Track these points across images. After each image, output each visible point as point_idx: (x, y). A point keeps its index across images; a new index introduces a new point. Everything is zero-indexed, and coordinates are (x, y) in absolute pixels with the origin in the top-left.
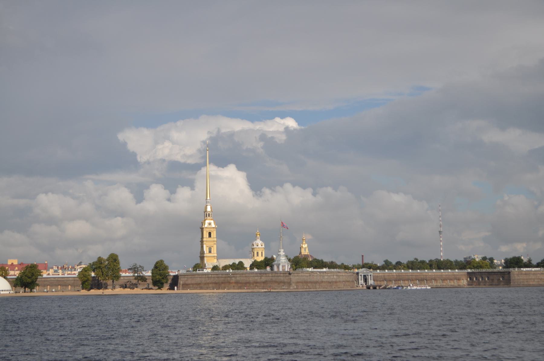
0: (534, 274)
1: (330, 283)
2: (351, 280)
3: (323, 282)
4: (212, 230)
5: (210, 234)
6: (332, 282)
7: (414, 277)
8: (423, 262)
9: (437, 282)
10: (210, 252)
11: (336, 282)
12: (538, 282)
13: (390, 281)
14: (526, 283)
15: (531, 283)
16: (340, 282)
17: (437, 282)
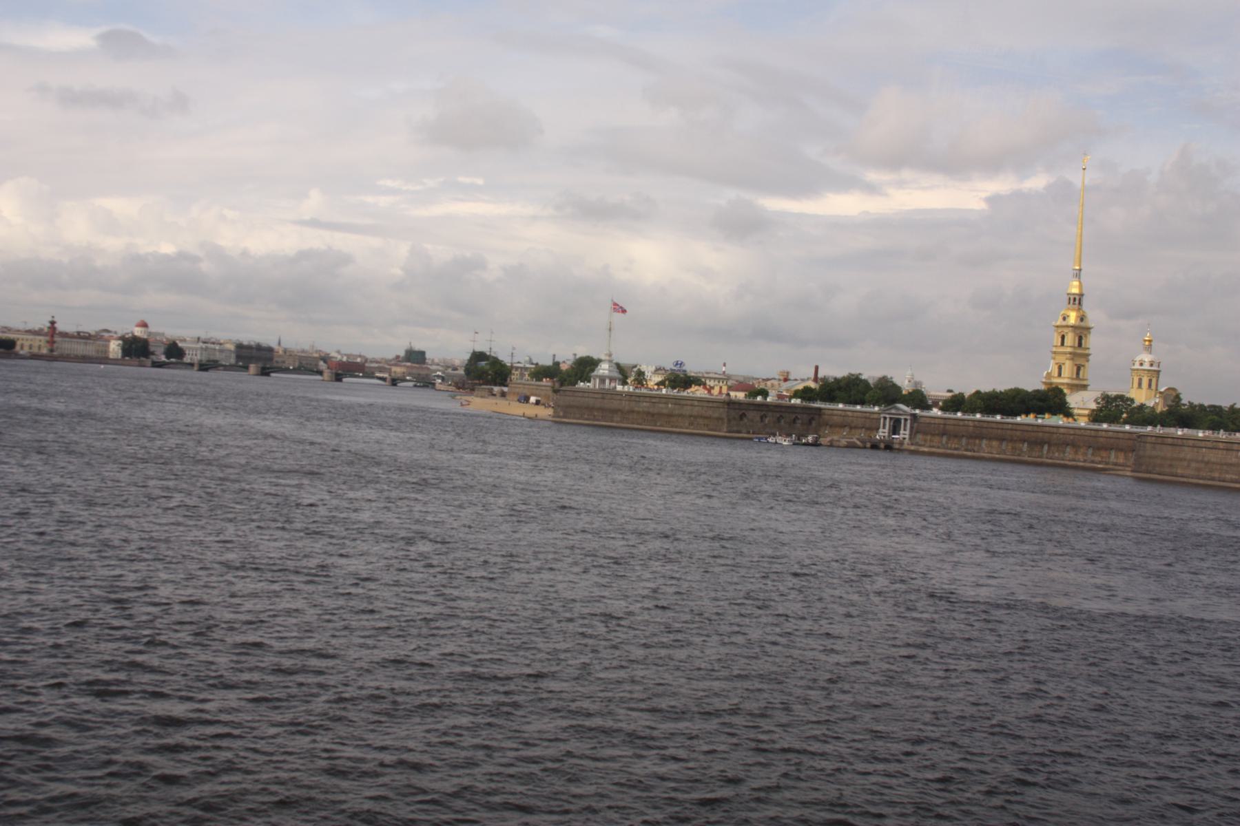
0: (1194, 446)
1: (653, 415)
2: (716, 415)
3: (633, 412)
4: (1066, 330)
5: (1063, 337)
6: (660, 415)
7: (1018, 433)
8: (1217, 410)
9: (1076, 452)
10: (1060, 375)
11: (670, 415)
12: (1198, 470)
13: (956, 436)
14: (1167, 470)
15: (1179, 471)
16: (680, 415)
17: (1076, 452)
